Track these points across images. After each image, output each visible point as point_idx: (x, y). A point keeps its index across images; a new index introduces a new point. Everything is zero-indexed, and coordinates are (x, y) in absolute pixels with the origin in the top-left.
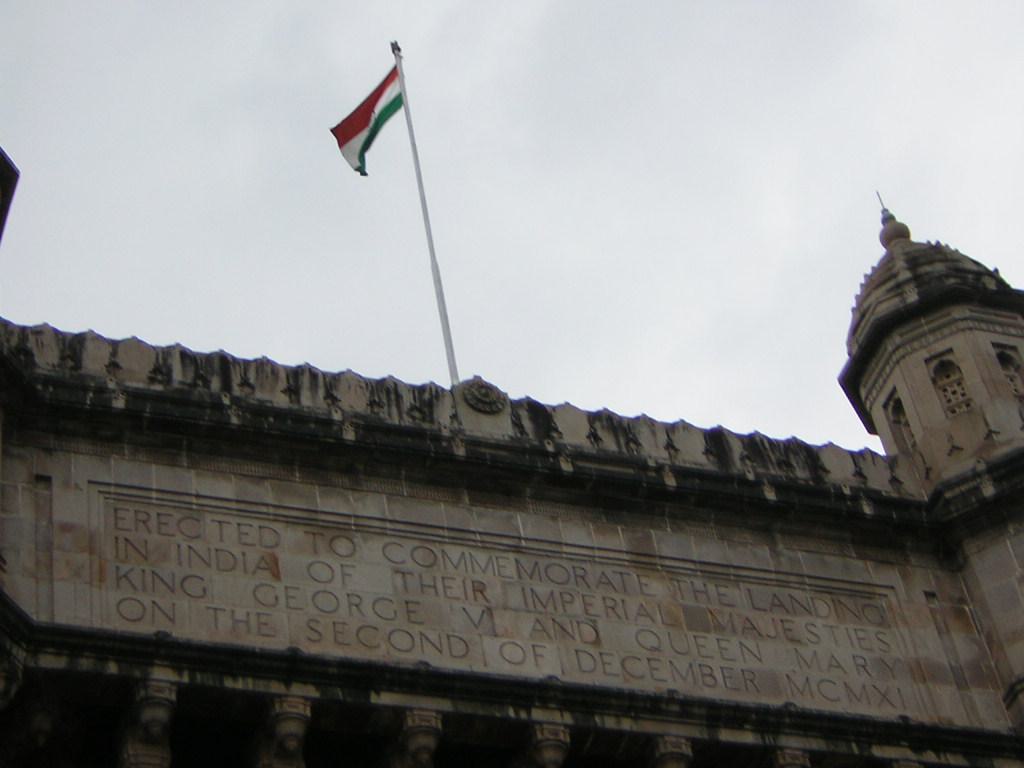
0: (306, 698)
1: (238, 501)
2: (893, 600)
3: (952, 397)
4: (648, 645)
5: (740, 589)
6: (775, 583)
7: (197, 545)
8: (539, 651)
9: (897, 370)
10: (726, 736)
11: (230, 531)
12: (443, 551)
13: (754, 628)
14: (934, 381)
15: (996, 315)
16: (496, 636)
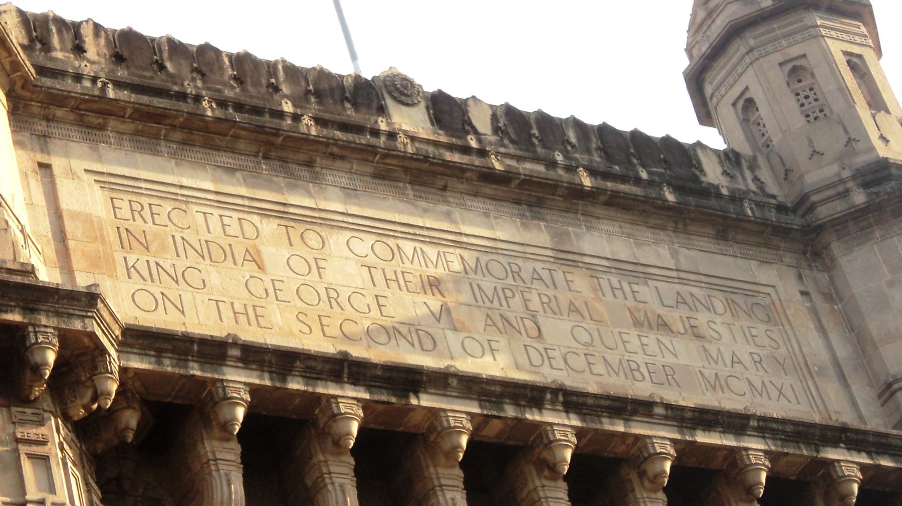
2: (774, 296)
3: (804, 101)
4: (583, 341)
5: (649, 286)
6: (677, 281)
9: (750, 72)
10: (703, 438)
11: (214, 221)
13: (666, 325)
14: (788, 84)
15: (841, 23)
16: (456, 330)
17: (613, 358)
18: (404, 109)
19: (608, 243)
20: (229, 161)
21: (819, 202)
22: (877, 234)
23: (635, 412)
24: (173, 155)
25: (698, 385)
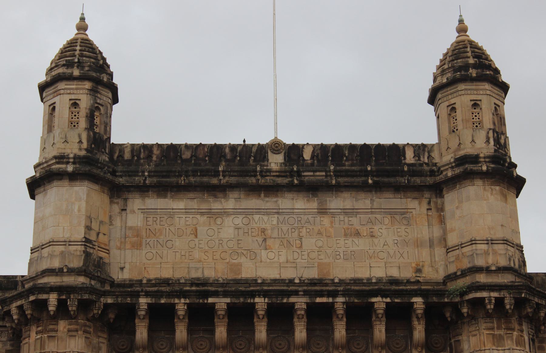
0: (185, 303)
1: (185, 209)
6: (370, 213)
7: (172, 228)
8: (280, 253)
10: (318, 300)
11: (183, 221)
12: (253, 217)
16: (266, 249)
17: (329, 251)
18: (275, 155)
19: (343, 201)
20: (192, 195)
21: (443, 170)
22: (458, 186)
23: (292, 295)
24: (172, 197)
25: (364, 257)
